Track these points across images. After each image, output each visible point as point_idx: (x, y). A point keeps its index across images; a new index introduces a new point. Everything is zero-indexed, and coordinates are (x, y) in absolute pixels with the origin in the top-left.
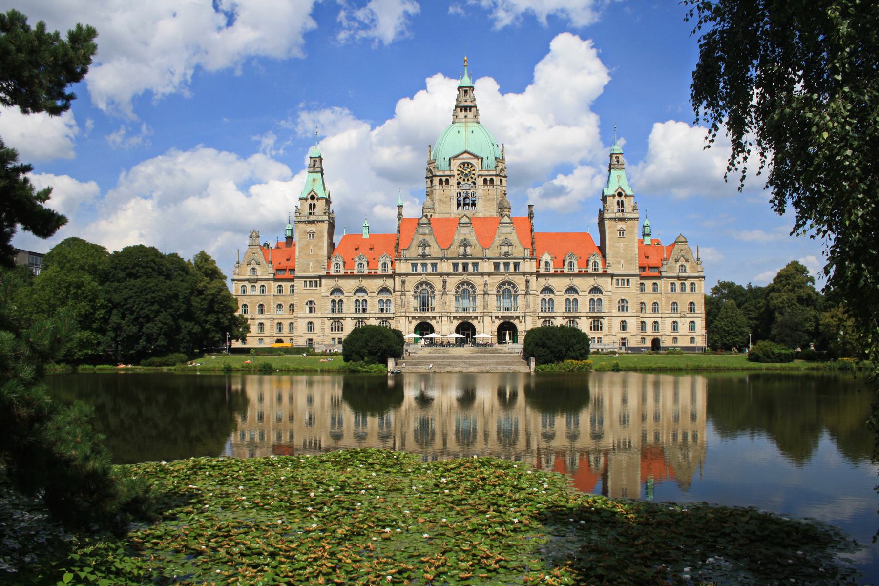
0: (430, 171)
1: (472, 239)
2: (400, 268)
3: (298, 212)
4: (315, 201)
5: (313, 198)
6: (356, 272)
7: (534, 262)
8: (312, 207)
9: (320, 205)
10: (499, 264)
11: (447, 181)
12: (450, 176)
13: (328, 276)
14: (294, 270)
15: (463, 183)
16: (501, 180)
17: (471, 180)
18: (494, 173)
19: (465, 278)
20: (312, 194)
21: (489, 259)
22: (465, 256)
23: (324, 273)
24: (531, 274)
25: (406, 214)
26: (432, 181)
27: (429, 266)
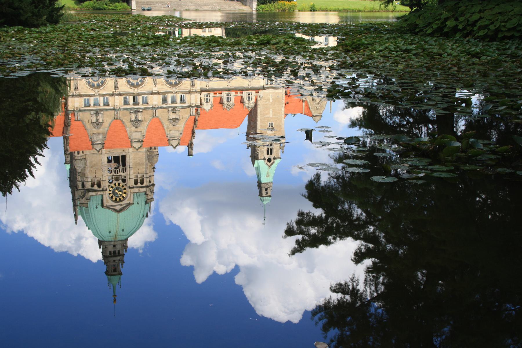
0: (152, 192)
1: (130, 128)
2: (196, 99)
3: (282, 148)
4: (267, 157)
5: (269, 160)
6: (233, 93)
7: (70, 108)
8: (270, 152)
9: (262, 153)
10: (104, 105)
11: (136, 182)
12: (133, 187)
13: (257, 90)
14: (286, 95)
15: (120, 181)
16: (83, 186)
17: (113, 185)
18: (91, 194)
19: (135, 91)
20: (269, 164)
21: (114, 109)
22: (136, 111)
23: (261, 92)
24: (73, 96)
25: (183, 149)
26: (150, 182)
27: (169, 100)
